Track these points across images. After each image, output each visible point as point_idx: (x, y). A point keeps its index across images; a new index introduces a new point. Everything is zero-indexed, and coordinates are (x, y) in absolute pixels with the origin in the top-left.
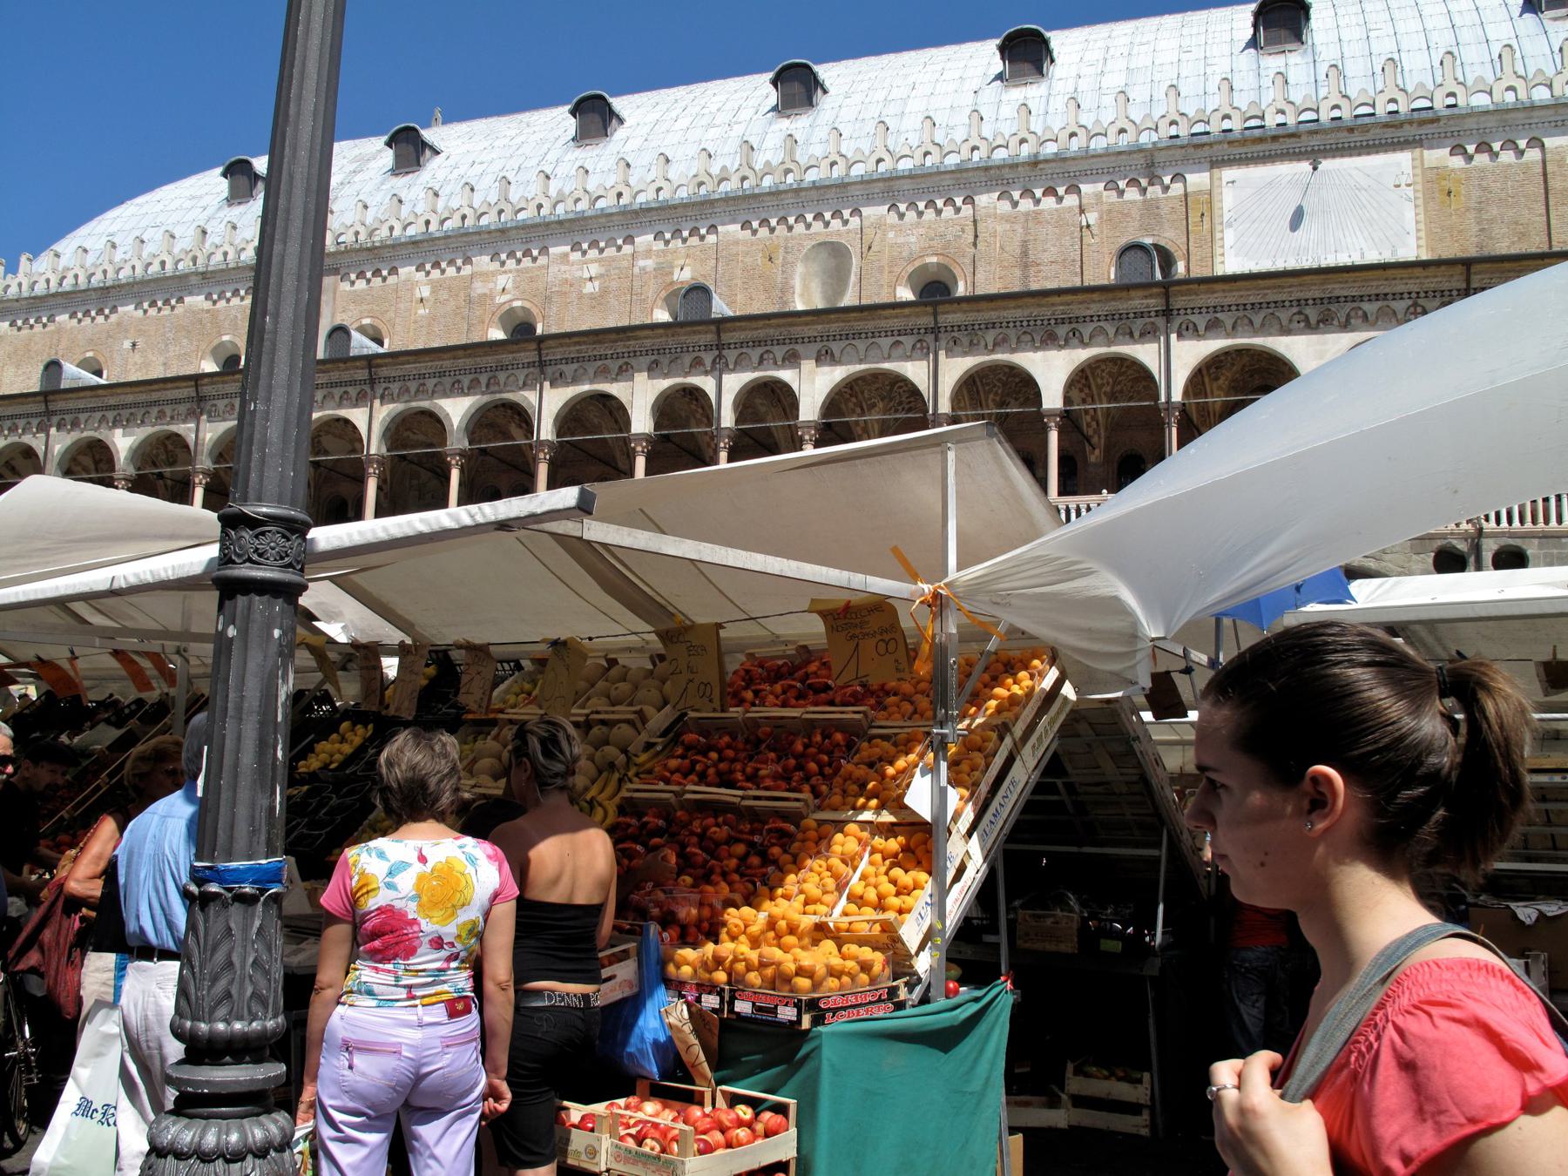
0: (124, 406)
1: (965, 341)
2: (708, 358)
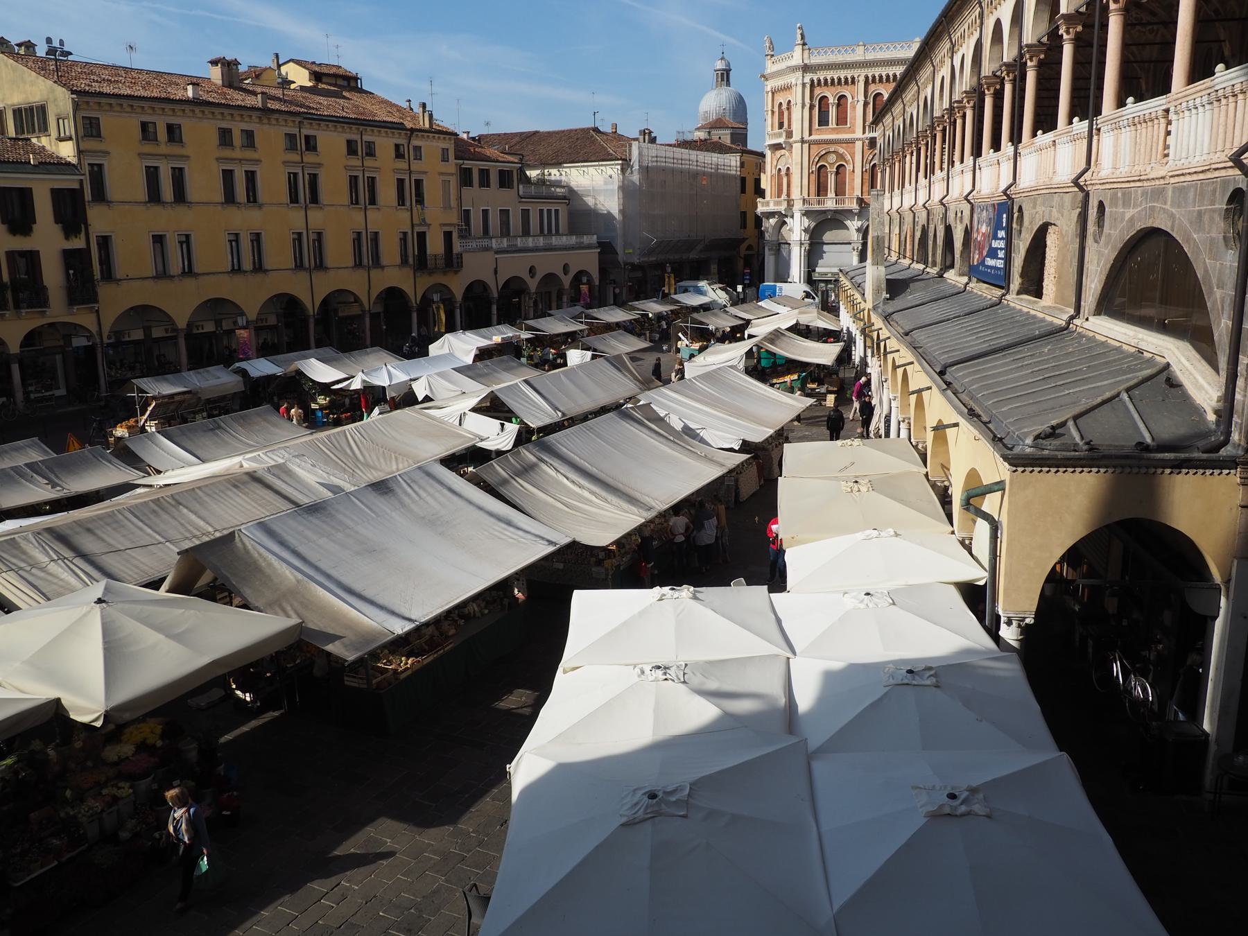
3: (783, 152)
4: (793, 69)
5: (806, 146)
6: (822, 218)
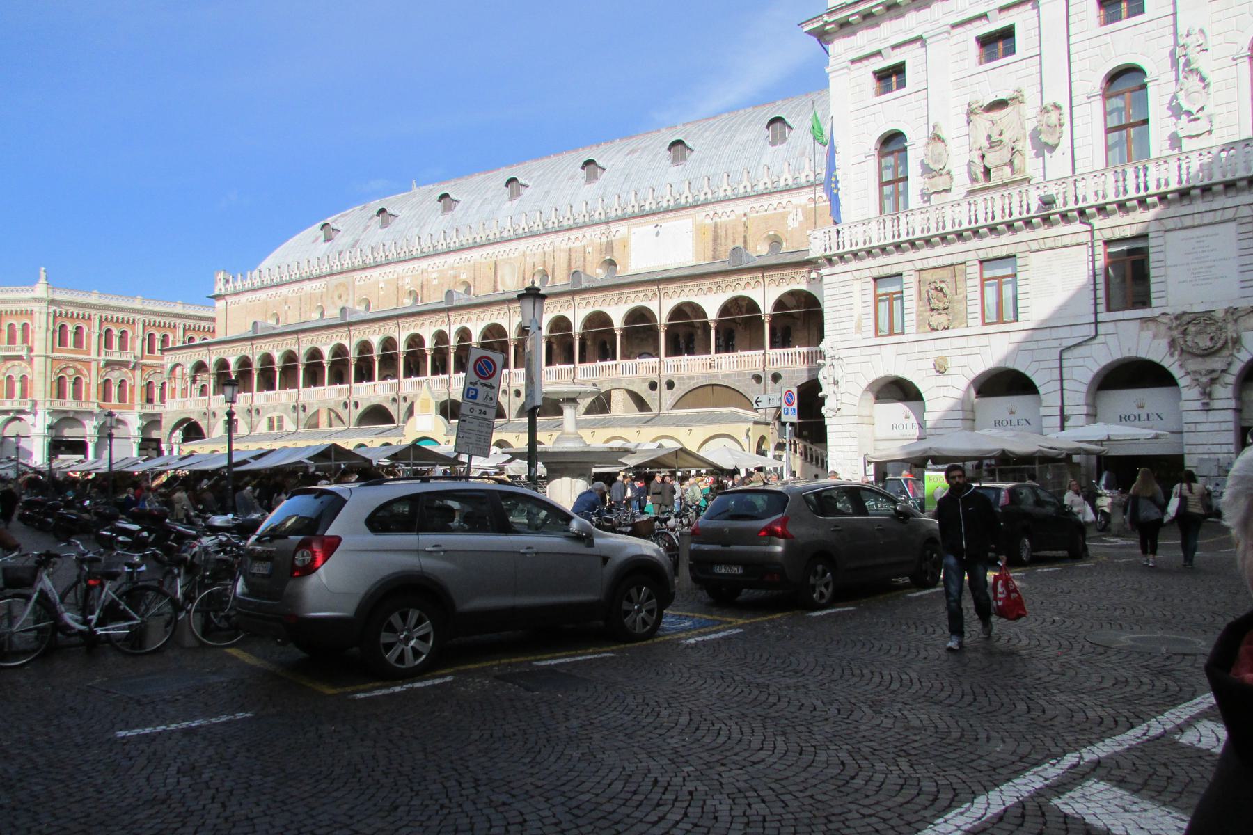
3: (17, 362)
4: (36, 300)
5: (49, 361)
6: (62, 416)
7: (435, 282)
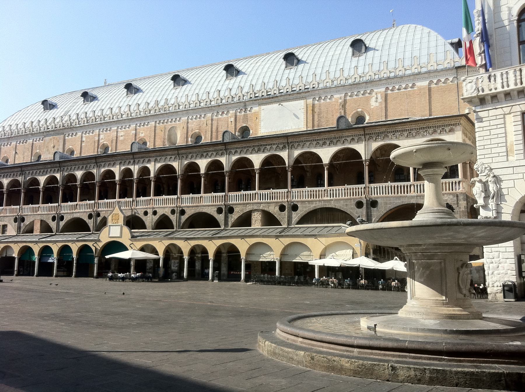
0: (5, 173)
1: (185, 157)
2: (132, 161)
7: (121, 138)
